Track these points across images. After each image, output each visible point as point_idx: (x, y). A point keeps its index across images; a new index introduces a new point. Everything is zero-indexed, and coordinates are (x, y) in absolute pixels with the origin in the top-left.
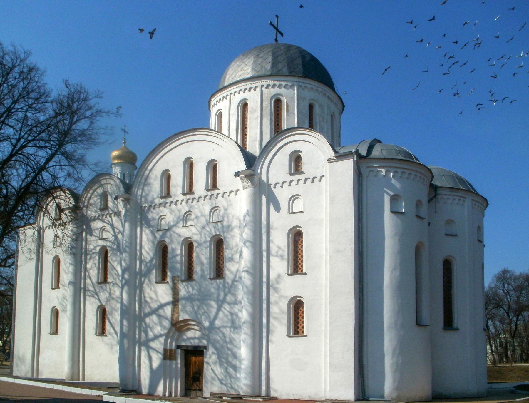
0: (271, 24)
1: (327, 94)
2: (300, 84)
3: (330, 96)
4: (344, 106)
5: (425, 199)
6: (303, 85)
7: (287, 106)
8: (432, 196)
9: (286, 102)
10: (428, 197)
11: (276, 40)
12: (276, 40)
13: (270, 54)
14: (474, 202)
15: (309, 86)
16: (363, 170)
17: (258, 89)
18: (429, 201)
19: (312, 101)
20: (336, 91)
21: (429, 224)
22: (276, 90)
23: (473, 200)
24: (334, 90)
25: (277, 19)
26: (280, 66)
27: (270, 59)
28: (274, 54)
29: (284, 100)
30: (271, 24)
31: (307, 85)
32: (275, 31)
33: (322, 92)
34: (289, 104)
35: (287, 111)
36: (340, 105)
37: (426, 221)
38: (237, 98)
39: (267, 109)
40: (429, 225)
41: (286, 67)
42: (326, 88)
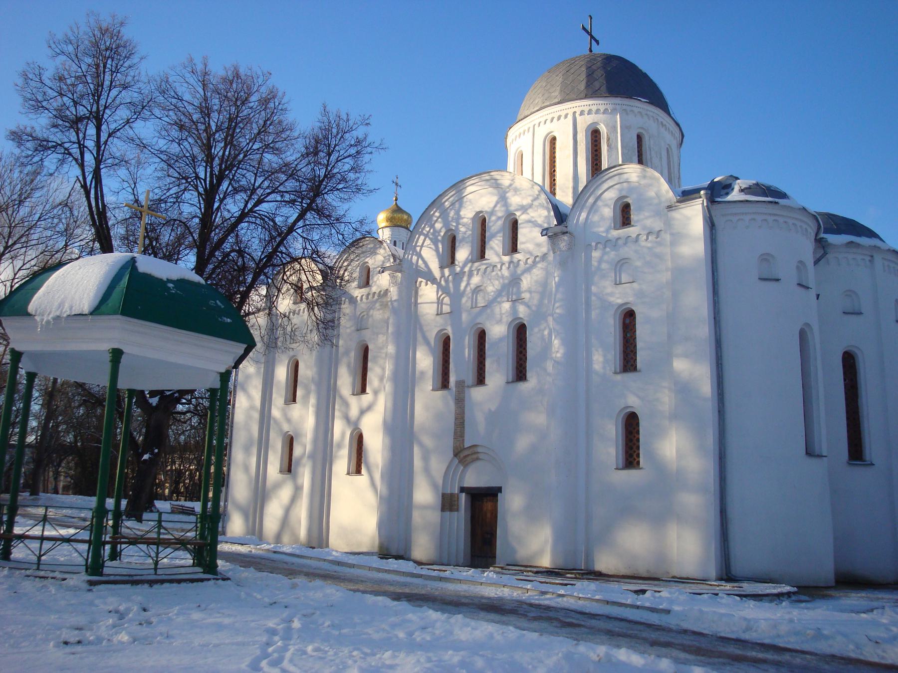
0: (584, 28)
1: (660, 119)
3: (665, 123)
4: (683, 136)
5: (809, 259)
6: (628, 108)
7: (608, 139)
8: (818, 256)
9: (607, 135)
10: (814, 257)
11: (591, 51)
12: (591, 51)
13: (584, 69)
14: (886, 263)
15: (636, 110)
16: (719, 221)
17: (570, 117)
18: (816, 262)
20: (672, 115)
21: (818, 296)
23: (883, 258)
24: (669, 114)
25: (591, 21)
26: (597, 84)
27: (583, 77)
28: (588, 68)
29: (603, 129)
30: (584, 28)
32: (589, 37)
33: (653, 117)
36: (678, 134)
37: (812, 294)
38: (541, 133)
39: (582, 144)
40: (818, 299)
41: (605, 85)
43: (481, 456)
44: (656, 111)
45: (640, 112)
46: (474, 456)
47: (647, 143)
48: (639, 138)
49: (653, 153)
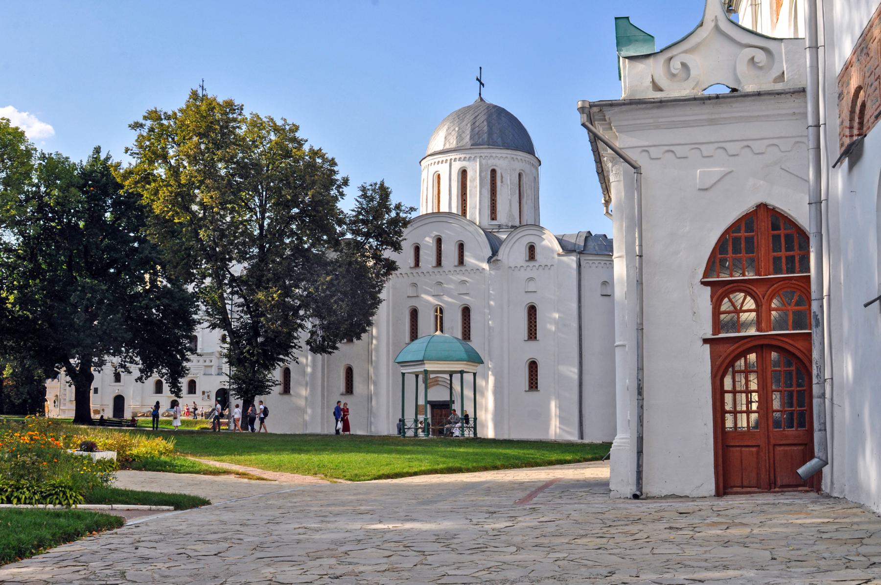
2: (513, 156)
4: (540, 165)
7: (502, 177)
11: (480, 94)
12: (480, 94)
13: (485, 123)
16: (583, 263)
19: (521, 171)
20: (536, 156)
22: (492, 163)
31: (518, 157)
34: (503, 176)
35: (502, 182)
38: (457, 166)
42: (530, 157)
43: (440, 383)
44: (529, 157)
45: (521, 159)
46: (436, 383)
47: (524, 180)
48: (520, 175)
49: (527, 185)
